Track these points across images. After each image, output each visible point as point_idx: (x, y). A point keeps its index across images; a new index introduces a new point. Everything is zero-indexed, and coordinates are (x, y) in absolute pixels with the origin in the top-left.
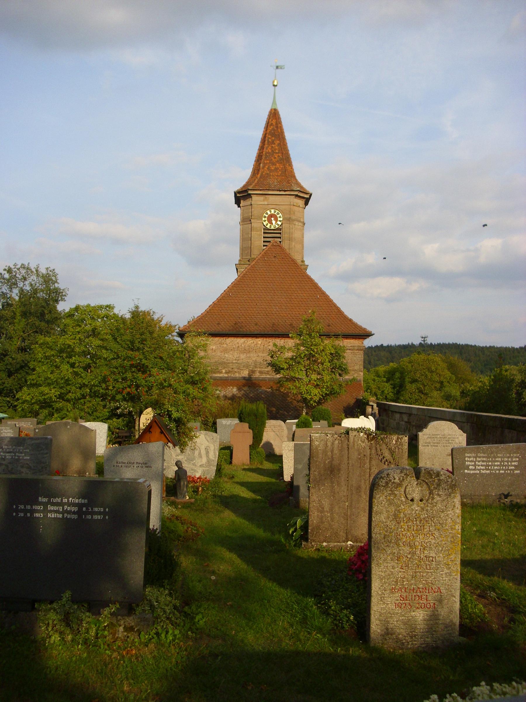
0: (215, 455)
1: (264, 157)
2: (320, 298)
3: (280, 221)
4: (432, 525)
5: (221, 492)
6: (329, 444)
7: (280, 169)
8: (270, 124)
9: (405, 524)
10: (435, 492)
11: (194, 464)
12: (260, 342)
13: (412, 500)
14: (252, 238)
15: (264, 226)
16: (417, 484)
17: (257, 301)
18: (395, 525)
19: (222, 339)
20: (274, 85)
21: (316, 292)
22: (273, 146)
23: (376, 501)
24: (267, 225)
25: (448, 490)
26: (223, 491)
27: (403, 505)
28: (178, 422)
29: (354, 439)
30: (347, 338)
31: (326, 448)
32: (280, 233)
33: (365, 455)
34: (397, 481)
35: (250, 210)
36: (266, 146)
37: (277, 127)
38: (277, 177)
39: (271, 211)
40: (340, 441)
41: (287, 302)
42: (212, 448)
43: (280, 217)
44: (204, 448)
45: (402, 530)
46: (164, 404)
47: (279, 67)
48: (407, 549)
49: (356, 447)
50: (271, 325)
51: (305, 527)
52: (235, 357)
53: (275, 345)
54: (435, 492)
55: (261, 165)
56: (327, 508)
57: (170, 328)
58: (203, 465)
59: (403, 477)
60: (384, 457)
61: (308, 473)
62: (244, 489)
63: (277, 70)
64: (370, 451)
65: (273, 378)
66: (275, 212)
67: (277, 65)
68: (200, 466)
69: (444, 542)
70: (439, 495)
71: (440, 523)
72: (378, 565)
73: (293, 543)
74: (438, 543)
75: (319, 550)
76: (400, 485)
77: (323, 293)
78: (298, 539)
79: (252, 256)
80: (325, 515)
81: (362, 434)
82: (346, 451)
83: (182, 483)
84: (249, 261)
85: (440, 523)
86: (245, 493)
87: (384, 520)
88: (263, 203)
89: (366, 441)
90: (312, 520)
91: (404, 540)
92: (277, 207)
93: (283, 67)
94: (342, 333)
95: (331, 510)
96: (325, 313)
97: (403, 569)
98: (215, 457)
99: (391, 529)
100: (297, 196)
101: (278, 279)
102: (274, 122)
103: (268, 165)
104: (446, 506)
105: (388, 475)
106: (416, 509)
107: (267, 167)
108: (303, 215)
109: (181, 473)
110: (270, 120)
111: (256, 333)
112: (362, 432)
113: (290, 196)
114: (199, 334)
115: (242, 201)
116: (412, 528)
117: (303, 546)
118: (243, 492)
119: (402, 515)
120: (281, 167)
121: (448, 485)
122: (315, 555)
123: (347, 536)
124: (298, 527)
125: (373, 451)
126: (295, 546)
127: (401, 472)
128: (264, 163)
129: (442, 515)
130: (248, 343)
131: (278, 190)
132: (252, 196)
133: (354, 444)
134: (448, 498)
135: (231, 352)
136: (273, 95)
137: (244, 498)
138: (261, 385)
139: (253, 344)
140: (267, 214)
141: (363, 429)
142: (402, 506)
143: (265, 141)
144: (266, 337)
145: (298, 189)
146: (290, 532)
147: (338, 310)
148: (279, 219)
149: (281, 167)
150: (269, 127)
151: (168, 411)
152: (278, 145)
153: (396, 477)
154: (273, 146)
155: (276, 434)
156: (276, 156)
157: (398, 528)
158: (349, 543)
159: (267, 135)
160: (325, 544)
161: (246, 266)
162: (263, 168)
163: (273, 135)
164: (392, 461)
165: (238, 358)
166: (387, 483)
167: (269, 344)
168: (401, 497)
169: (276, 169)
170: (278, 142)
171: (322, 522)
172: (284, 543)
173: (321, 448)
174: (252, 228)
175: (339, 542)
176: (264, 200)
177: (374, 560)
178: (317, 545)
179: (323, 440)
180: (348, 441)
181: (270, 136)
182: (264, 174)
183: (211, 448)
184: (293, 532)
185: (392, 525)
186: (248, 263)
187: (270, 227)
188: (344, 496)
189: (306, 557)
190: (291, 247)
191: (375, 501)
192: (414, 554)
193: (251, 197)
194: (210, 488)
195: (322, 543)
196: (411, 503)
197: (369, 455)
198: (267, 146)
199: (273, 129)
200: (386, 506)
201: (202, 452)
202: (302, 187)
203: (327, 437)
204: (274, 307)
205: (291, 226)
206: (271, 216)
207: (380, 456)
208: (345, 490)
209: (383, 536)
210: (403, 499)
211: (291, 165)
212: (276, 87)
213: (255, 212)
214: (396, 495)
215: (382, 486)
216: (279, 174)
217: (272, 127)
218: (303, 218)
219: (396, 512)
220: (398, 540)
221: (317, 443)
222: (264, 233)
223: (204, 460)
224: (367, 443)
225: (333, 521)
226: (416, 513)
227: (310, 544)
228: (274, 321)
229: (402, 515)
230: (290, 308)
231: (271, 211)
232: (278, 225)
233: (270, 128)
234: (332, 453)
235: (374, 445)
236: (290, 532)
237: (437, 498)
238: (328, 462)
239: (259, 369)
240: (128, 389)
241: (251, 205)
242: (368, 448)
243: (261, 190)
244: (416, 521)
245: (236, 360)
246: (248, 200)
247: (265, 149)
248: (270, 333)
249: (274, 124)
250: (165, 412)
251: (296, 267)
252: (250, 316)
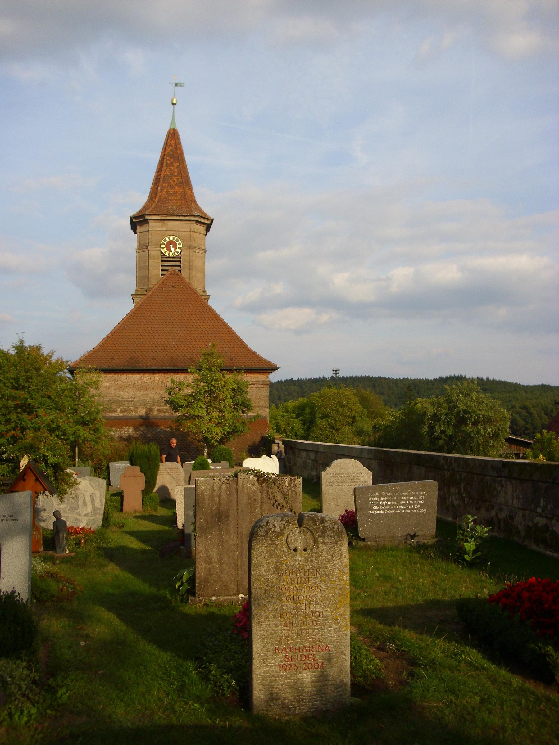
0: (101, 502)
2: (222, 330)
3: (179, 248)
4: (317, 577)
5: (107, 544)
6: (216, 488)
7: (179, 192)
8: (168, 144)
9: (288, 577)
10: (320, 540)
11: (78, 514)
12: (158, 378)
13: (295, 550)
14: (149, 267)
15: (162, 253)
16: (300, 532)
17: (154, 334)
18: (277, 579)
19: (116, 375)
20: (173, 104)
21: (218, 324)
22: (172, 168)
23: (255, 553)
24: (165, 252)
25: (334, 537)
26: (109, 542)
27: (285, 556)
28: (56, 468)
29: (243, 482)
30: (251, 373)
31: (212, 493)
32: (180, 261)
33: (255, 500)
34: (278, 529)
36: (164, 168)
37: (176, 148)
38: (176, 202)
39: (169, 238)
40: (228, 485)
41: (186, 335)
42: (98, 494)
43: (179, 244)
44: (89, 495)
45: (285, 583)
46: (39, 448)
47: (179, 85)
48: (291, 605)
49: (245, 491)
50: (170, 360)
51: (192, 580)
52: (131, 394)
53: (173, 381)
54: (320, 540)
55: (159, 188)
56: (215, 558)
57: (60, 364)
58: (88, 514)
59: (284, 525)
60: (276, 501)
61: (194, 521)
62: (133, 539)
63: (177, 87)
64: (261, 495)
65: (173, 416)
66: (174, 238)
67: (177, 82)
68: (85, 515)
69: (331, 595)
70: (324, 543)
71: (326, 575)
72: (260, 623)
73: (179, 599)
74: (325, 596)
75: (207, 605)
76: (281, 534)
77: (225, 325)
78: (184, 594)
80: (213, 566)
81: (251, 477)
82: (235, 496)
83: (61, 536)
84: (146, 291)
85: (326, 575)
86: (134, 544)
87: (265, 574)
88: (162, 229)
89: (257, 484)
90: (199, 573)
91: (287, 595)
92: (177, 233)
94: (245, 367)
95: (220, 560)
96: (227, 346)
97: (287, 626)
98: (102, 505)
99: (273, 582)
100: (197, 221)
101: (177, 311)
102: (173, 142)
103: (166, 188)
104: (332, 556)
105: (267, 523)
106: (300, 559)
107: (165, 190)
108: (204, 242)
109: (59, 524)
110: (169, 141)
111: (153, 368)
112: (251, 475)
113: (190, 222)
114: (90, 371)
115: (138, 227)
116: (296, 581)
117: (190, 602)
118: (131, 542)
119: (284, 567)
120: (181, 190)
121: (333, 532)
122: (203, 611)
123: (237, 587)
124: (184, 581)
125: (265, 495)
126: (182, 601)
127: (282, 519)
128: (162, 186)
129: (328, 565)
130: (145, 379)
131: (177, 216)
132: (149, 221)
133: (243, 488)
134: (334, 546)
135: (126, 389)
136: (172, 114)
137: (132, 549)
138: (159, 424)
139: (151, 380)
140: (165, 240)
141: (253, 471)
142: (284, 557)
143: (163, 163)
144: (164, 373)
145: (199, 214)
146: (177, 586)
147: (241, 342)
148: (178, 246)
149: (181, 190)
151: (44, 456)
152: (177, 167)
153: (277, 525)
154: (172, 168)
155: (173, 477)
156: (175, 179)
157: (280, 582)
158: (241, 595)
160: (214, 598)
161: (143, 296)
162: (162, 191)
163: (171, 156)
164: (285, 505)
165: (133, 396)
166: (266, 532)
167: (168, 380)
168: (282, 547)
169: (175, 193)
170: (177, 164)
171: (211, 575)
172: (170, 599)
173: (207, 492)
174: (150, 256)
175: (229, 596)
176: (162, 226)
177: (254, 618)
178: (205, 599)
179: (208, 484)
180: (237, 485)
181: (168, 158)
182: (162, 198)
183: (97, 495)
184: (179, 586)
185: (273, 578)
186: (145, 293)
187: (169, 254)
188: (234, 545)
189: (192, 614)
190: (191, 276)
191: (254, 552)
192: (298, 609)
193: (149, 223)
194: (95, 540)
195: (212, 597)
196: (294, 553)
197: (259, 499)
198: (165, 168)
199: (172, 150)
200: (266, 557)
201: (86, 499)
202: (203, 212)
203: (214, 481)
204: (172, 340)
205: (191, 254)
206: (170, 243)
207: (271, 500)
208: (235, 539)
209: (263, 591)
210: (285, 549)
211: (191, 189)
212: (175, 106)
213: (153, 238)
214: (277, 545)
215: (261, 535)
216: (178, 199)
217: (170, 148)
218: (204, 245)
219: (278, 564)
220: (280, 595)
221: (202, 488)
222: (162, 261)
223: (89, 508)
224: (257, 486)
225: (222, 573)
226: (299, 564)
227: (198, 599)
228: (172, 355)
229: (284, 567)
230: (190, 340)
231: (169, 238)
232: (177, 252)
233: (169, 149)
234: (219, 498)
235: (265, 488)
236: (177, 586)
237: (323, 547)
238: (216, 508)
239: (157, 408)
240: (13, 432)
241: (148, 231)
242: (259, 492)
243: (159, 215)
244: (300, 573)
245: (132, 397)
246: (144, 226)
247: (163, 172)
248: (168, 368)
249: (173, 145)
250: (40, 457)
251: (195, 298)
252: (146, 351)
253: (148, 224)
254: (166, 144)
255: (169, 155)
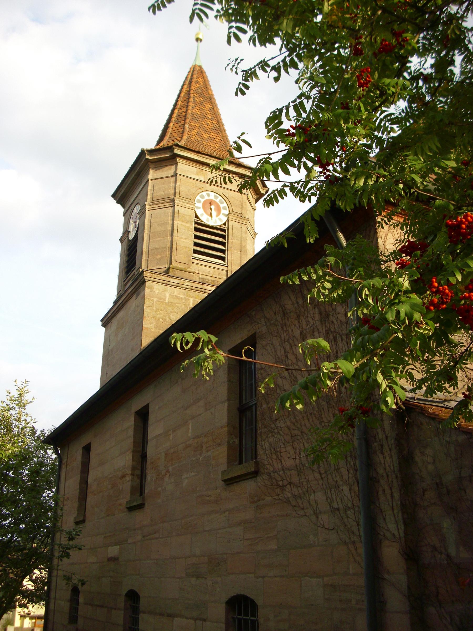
1: (189, 116)
8: (194, 80)
15: (196, 216)
20: (197, 40)
32: (223, 237)
35: (172, 185)
36: (191, 104)
55: (187, 126)
79: (174, 264)
93: (208, 27)
110: (195, 76)
115: (151, 171)
128: (190, 125)
132: (179, 160)
143: (189, 99)
148: (223, 211)
150: (193, 84)
159: (192, 92)
162: (190, 131)
163: (200, 95)
174: (176, 215)
176: (197, 174)
193: (176, 164)
222: (196, 230)
232: (220, 220)
241: (175, 175)
246: (167, 168)
247: (190, 108)
253: (173, 167)
254: (191, 79)
255: (196, 91)
